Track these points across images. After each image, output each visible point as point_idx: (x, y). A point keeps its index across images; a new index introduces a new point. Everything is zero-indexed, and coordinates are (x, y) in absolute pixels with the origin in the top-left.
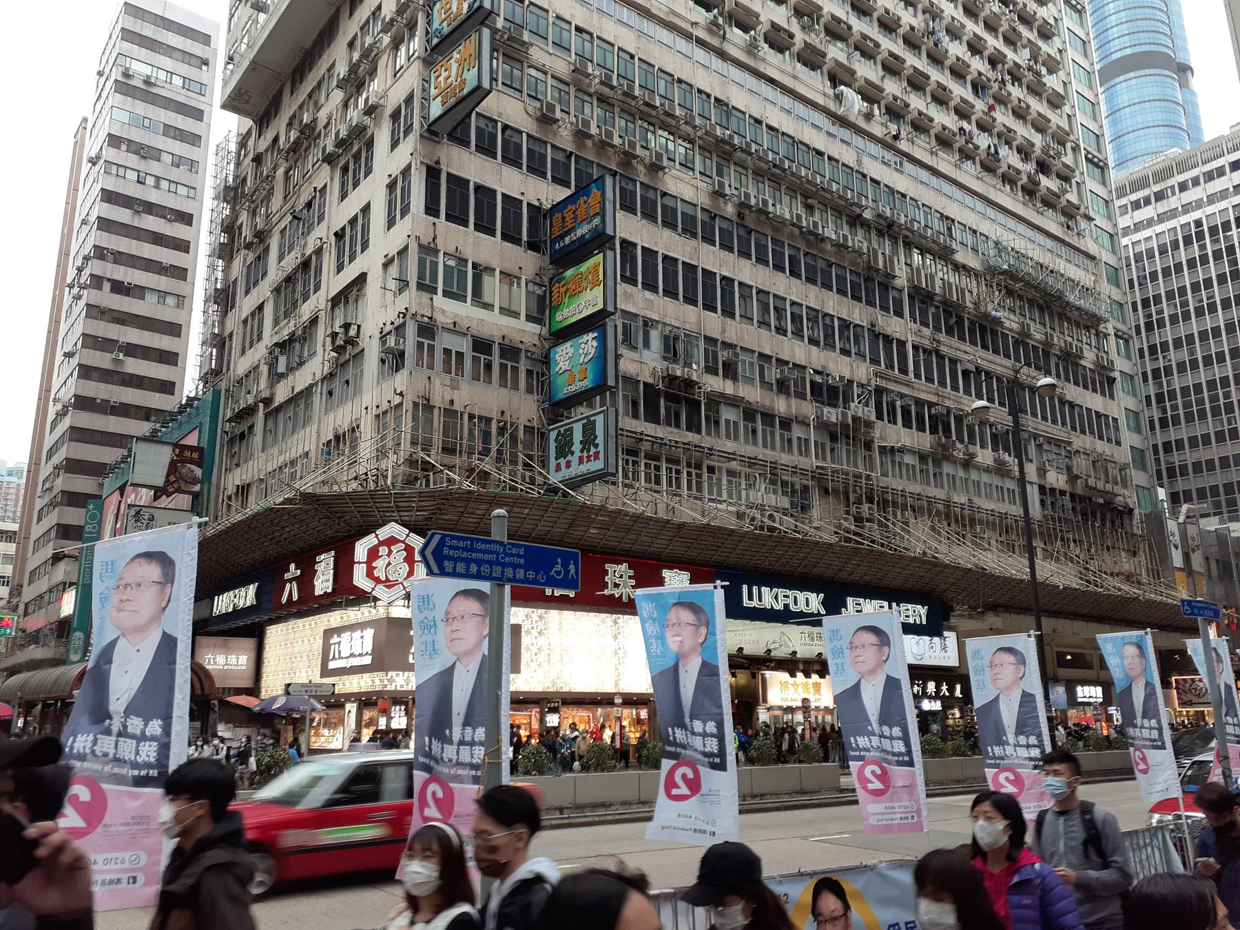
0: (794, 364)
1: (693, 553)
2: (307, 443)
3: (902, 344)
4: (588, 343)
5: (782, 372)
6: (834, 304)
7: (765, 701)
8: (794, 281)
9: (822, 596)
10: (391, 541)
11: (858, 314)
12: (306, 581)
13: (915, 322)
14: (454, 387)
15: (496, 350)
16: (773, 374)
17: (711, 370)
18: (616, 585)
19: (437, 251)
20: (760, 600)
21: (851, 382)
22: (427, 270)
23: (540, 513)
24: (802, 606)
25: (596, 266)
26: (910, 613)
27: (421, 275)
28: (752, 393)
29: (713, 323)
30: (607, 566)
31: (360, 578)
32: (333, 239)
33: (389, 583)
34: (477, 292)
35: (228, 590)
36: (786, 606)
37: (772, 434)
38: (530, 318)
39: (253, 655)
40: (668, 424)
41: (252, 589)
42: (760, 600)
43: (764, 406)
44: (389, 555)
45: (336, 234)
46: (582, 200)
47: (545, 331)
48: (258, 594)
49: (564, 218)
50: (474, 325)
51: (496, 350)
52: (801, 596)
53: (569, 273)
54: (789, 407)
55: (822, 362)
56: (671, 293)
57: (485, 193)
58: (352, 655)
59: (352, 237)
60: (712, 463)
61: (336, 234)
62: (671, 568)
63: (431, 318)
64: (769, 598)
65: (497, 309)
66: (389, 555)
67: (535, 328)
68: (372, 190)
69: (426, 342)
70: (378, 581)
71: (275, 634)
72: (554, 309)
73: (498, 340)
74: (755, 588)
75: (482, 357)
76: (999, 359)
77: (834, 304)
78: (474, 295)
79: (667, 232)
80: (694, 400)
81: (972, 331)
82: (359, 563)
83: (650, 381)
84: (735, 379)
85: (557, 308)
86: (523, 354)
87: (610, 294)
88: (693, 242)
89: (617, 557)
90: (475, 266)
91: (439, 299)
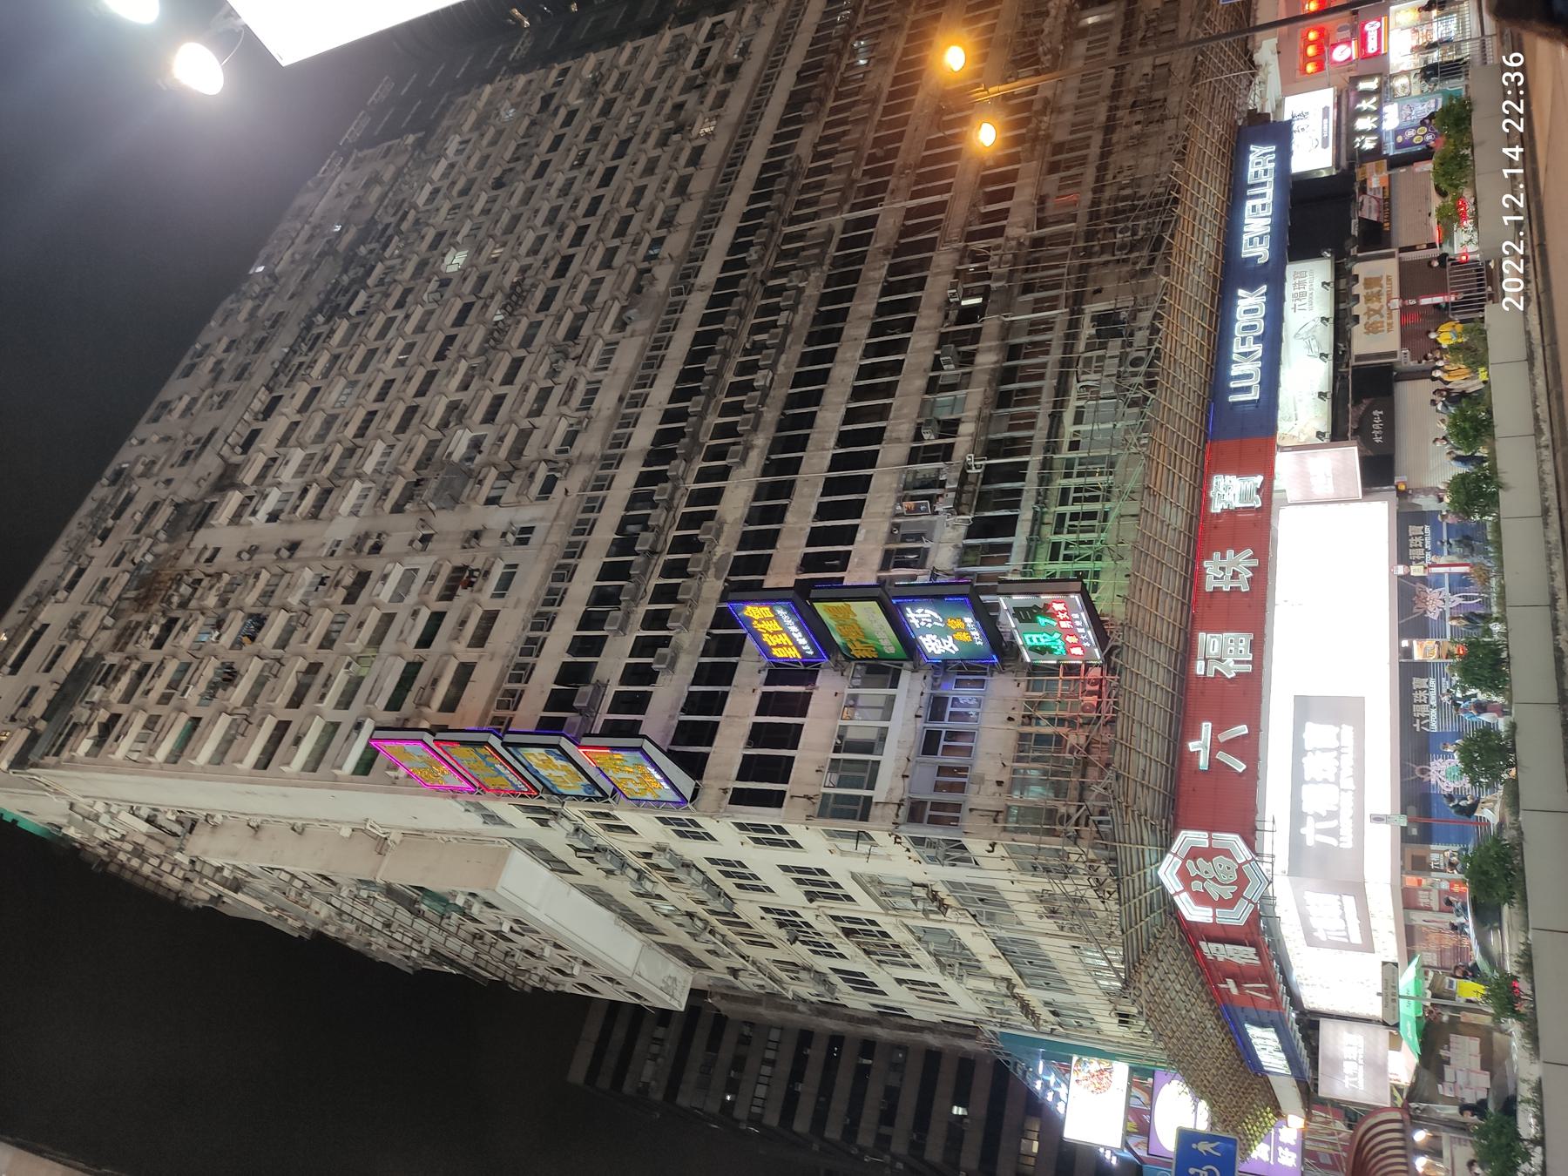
0: (938, 348)
1: (1187, 471)
3: (910, 213)
4: (919, 616)
5: (948, 363)
6: (864, 306)
7: (1394, 354)
8: (839, 356)
9: (1241, 292)
10: (1184, 875)
11: (875, 273)
12: (1241, 975)
13: (882, 199)
14: (981, 780)
16: (950, 371)
17: (946, 453)
18: (1235, 575)
20: (1249, 376)
21: (957, 274)
22: (847, 809)
23: (1140, 683)
25: (828, 610)
26: (1260, 169)
27: (851, 816)
28: (974, 398)
29: (892, 453)
31: (1237, 917)
32: (815, 904)
33: (1242, 881)
34: (867, 747)
35: (1256, 1055)
36: (1257, 339)
37: (1024, 367)
38: (894, 685)
39: (1342, 1025)
41: (1254, 1032)
43: (990, 383)
44: (1203, 880)
45: (811, 901)
46: (758, 627)
47: (907, 665)
48: (1262, 1025)
49: (778, 646)
50: (905, 753)
52: (1241, 319)
53: (838, 639)
54: (989, 349)
55: (933, 312)
56: (856, 509)
57: (758, 735)
58: (1343, 917)
59: (816, 884)
60: (1066, 446)
61: (811, 901)
62: (1208, 501)
64: (1245, 367)
66: (1203, 880)
67: (905, 677)
68: (763, 861)
69: (928, 812)
70: (1238, 895)
71: (1313, 999)
72: (882, 656)
73: (920, 723)
74: (1233, 385)
75: (942, 743)
77: (864, 306)
78: (870, 752)
79: (790, 517)
80: (985, 473)
81: (891, 125)
82: (1214, 916)
83: (963, 530)
85: (880, 652)
86: (939, 692)
87: (861, 593)
88: (798, 484)
90: (837, 750)
91: (878, 794)
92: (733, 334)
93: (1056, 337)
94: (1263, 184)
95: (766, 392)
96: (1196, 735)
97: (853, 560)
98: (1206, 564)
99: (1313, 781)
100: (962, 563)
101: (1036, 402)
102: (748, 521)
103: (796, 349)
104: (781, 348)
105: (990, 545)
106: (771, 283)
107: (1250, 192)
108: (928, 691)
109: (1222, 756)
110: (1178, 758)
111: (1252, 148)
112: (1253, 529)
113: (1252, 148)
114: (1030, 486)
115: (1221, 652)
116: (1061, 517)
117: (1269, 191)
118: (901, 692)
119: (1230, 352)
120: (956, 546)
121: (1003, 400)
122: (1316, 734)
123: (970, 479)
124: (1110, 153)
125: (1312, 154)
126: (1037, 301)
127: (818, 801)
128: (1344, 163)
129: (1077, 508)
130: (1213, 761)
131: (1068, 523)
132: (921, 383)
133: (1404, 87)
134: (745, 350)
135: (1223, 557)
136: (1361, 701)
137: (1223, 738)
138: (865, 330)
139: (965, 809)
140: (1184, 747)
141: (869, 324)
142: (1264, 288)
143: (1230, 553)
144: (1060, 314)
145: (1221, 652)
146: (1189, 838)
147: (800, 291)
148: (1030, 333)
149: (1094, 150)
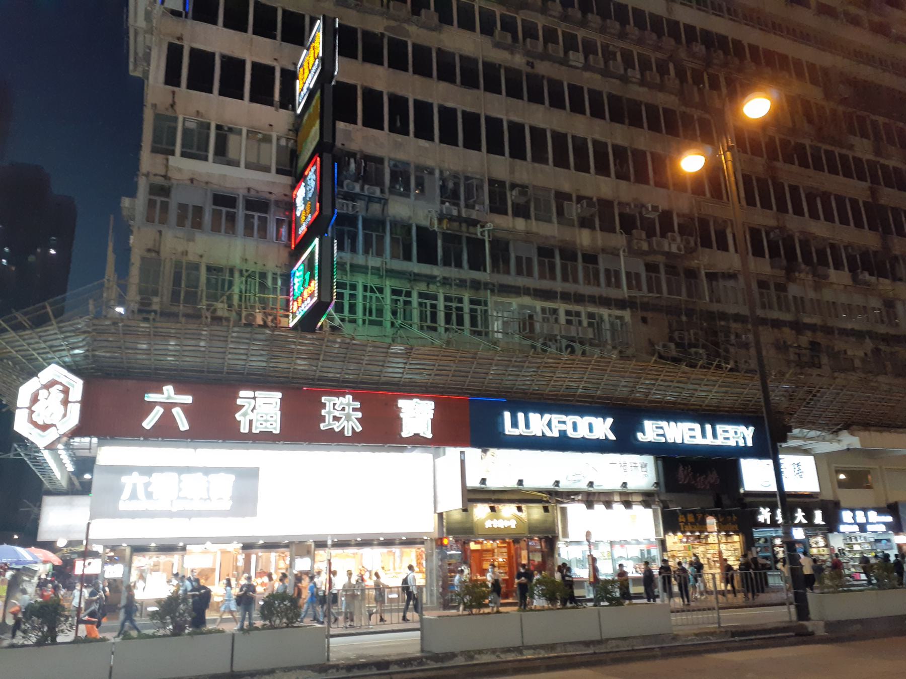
1: (439, 380)
2: (378, 358)
7: (565, 535)
9: (610, 421)
14: (191, 239)
15: (241, 204)
16: (574, 210)
18: (336, 419)
19: (175, 119)
20: (527, 426)
24: (583, 432)
28: (550, 231)
29: (500, 167)
30: (324, 399)
38: (279, 172)
40: (446, 263)
42: (527, 426)
51: (241, 204)
62: (410, 397)
63: (165, 177)
64: (538, 424)
65: (242, 164)
70: (35, 424)
73: (242, 192)
74: (521, 416)
75: (224, 210)
76: (854, 182)
79: (443, 86)
83: (425, 223)
84: (527, 216)
88: (475, 92)
89: (338, 388)
90: (219, 127)
92: (623, 36)
93: (603, 290)
94: (715, 436)
95: (564, 62)
96: (178, 391)
97: (399, 138)
98: (349, 398)
99: (180, 481)
100: (395, 224)
101: (542, 276)
102: (440, 51)
103: (606, 86)
104: (606, 73)
105: (410, 245)
106: (671, 66)
107: (708, 427)
108: (273, 198)
109: (158, 412)
110: (156, 378)
111: (752, 429)
112: (381, 431)
113: (752, 429)
114: (468, 274)
115: (261, 409)
116: (435, 298)
117: (709, 441)
118: (272, 177)
119: (551, 411)
120: (410, 218)
121: (545, 252)
122: (225, 485)
123: (472, 229)
124: (773, 326)
125: (756, 475)
126: (638, 275)
127: (170, 113)
128: (748, 500)
129: (415, 304)
130: (155, 404)
131: (428, 302)
132: (566, 187)
133: (817, 543)
134: (608, 46)
135: (354, 410)
136: (254, 514)
137: (177, 412)
138: (619, 141)
139: (161, 227)
140: (168, 381)
141: (625, 144)
142: (612, 437)
143: (359, 415)
144: (624, 292)
145: (261, 409)
146: (77, 386)
147: (661, 88)
148: (607, 271)
149: (776, 314)
